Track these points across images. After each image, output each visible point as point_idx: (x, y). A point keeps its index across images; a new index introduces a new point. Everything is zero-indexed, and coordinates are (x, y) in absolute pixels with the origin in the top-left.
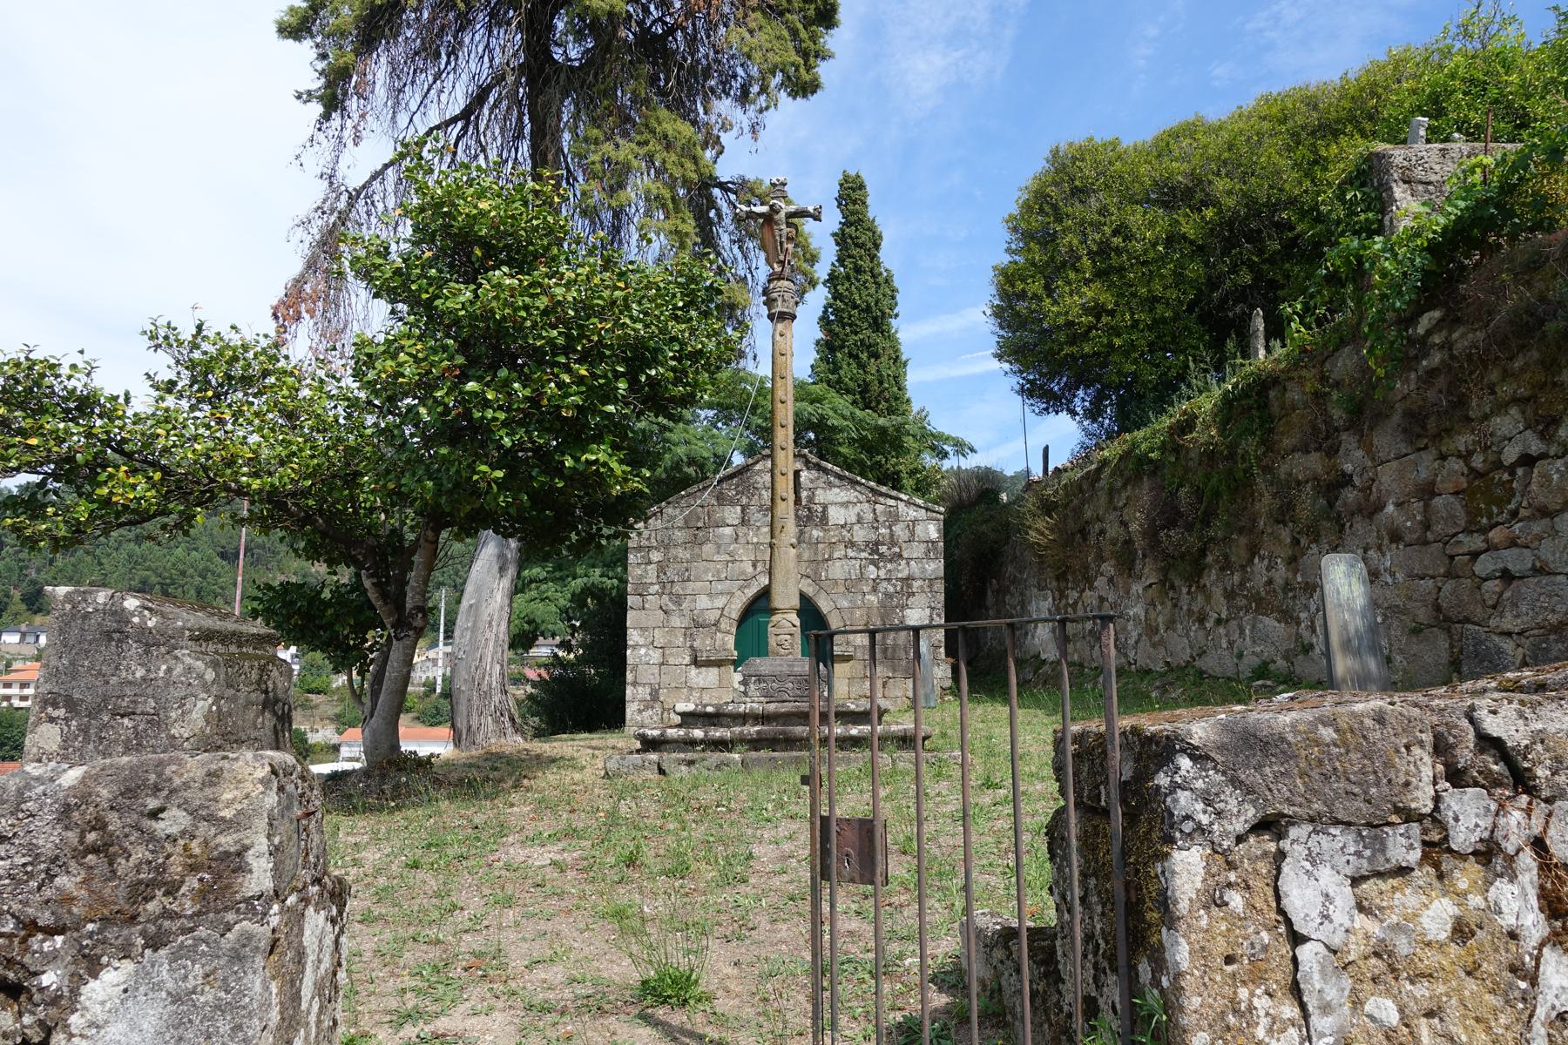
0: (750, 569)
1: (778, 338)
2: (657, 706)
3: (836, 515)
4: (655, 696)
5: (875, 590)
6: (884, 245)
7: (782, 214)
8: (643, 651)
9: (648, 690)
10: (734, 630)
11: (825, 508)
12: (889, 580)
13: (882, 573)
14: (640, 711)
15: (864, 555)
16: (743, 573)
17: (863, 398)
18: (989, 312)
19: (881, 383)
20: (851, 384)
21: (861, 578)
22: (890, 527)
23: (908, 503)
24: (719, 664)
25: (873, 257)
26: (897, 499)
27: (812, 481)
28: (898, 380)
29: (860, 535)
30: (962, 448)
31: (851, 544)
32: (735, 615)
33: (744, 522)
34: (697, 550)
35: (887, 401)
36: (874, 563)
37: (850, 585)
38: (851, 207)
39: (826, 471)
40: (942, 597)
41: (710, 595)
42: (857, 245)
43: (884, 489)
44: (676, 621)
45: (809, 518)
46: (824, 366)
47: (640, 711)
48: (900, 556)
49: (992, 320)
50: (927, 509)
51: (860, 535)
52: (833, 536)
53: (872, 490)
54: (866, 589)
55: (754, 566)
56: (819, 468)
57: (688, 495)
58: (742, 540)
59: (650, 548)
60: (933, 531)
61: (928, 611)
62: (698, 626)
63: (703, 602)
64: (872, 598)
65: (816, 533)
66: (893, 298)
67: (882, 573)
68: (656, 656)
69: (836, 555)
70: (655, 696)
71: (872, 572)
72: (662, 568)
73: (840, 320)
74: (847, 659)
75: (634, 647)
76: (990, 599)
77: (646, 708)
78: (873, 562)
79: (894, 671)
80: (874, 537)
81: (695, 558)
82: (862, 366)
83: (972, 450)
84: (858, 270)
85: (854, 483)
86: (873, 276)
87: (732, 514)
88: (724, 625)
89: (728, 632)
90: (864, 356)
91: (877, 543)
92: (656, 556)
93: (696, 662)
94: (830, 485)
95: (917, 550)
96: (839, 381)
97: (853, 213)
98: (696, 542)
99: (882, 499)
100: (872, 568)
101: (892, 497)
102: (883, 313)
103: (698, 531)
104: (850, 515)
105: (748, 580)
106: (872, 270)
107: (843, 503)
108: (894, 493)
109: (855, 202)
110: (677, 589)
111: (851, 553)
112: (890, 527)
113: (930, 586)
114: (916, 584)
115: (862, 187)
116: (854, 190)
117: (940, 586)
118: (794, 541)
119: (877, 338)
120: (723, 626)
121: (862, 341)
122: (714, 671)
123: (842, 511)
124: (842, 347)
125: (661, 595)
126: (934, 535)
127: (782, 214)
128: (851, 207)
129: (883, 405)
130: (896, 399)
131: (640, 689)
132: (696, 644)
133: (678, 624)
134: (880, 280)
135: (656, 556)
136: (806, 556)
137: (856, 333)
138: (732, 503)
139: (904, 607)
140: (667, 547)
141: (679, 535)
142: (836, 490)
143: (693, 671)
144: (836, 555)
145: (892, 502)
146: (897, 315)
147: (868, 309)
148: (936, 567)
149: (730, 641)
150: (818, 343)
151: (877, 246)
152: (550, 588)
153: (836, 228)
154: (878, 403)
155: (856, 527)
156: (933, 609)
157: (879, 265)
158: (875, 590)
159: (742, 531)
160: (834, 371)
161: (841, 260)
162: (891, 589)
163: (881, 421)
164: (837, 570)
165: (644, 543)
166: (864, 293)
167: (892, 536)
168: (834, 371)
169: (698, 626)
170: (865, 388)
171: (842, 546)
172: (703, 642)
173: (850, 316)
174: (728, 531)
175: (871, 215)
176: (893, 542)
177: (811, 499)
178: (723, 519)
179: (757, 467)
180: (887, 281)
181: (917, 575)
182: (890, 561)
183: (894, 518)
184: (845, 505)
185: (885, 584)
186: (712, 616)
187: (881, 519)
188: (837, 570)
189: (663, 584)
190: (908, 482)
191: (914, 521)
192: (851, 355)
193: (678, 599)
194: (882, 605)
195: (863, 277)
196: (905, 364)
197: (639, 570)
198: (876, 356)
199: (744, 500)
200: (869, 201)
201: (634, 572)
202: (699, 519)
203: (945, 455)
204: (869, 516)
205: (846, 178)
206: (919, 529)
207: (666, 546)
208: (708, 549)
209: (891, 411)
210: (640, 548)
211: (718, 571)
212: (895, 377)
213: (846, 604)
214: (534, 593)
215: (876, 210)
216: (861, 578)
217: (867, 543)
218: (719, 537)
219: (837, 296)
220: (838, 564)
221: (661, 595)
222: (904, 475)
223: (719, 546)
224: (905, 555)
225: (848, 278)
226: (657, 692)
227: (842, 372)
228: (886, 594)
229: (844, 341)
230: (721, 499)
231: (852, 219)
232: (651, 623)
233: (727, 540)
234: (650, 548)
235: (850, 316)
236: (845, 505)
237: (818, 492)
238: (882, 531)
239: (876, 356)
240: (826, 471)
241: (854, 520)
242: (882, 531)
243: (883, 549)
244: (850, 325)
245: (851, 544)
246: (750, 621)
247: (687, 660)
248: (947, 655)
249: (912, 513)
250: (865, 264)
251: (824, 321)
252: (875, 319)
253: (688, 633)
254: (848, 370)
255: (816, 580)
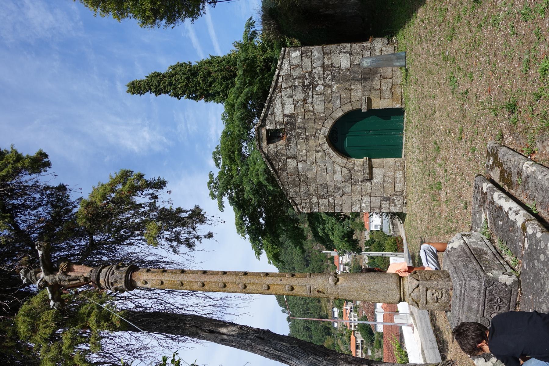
0: (320, 153)
1: (148, 286)
2: (392, 197)
3: (289, 109)
4: (387, 199)
5: (330, 86)
6: (158, 71)
7: (47, 278)
8: (364, 205)
9: (384, 202)
10: (354, 159)
11: (285, 116)
12: (324, 78)
13: (321, 82)
14: (395, 206)
15: (310, 93)
16: (322, 157)
17: (230, 79)
18: (172, 25)
19: (222, 70)
20: (224, 85)
21: (323, 94)
22: (294, 79)
23: (280, 69)
24: (371, 168)
25: (164, 77)
26: (278, 76)
27: (271, 123)
28: (220, 61)
29: (299, 96)
30: (250, 24)
31: (305, 100)
32: (345, 160)
33: (295, 157)
34: (311, 180)
35: (230, 67)
36: (315, 87)
37: (328, 100)
38: (142, 89)
39: (266, 116)
40: (334, 47)
41: (334, 173)
42: (159, 85)
43: (273, 84)
44: (348, 189)
45: (291, 124)
46: (217, 98)
47: (395, 206)
48: (310, 72)
49: (177, 23)
50: (283, 58)
51: (299, 96)
52: (300, 110)
53: (274, 90)
54: (330, 91)
55: (318, 151)
56: (264, 120)
57: (283, 185)
58: (305, 158)
59: (310, 202)
60: (296, 54)
61: (342, 55)
62: (350, 178)
63: (338, 176)
64: (335, 88)
65: (299, 120)
66: (182, 65)
67: (321, 82)
68: (366, 199)
69: (311, 109)
70: (387, 199)
71: (320, 88)
72: (322, 197)
73: (195, 91)
74: (369, 101)
75: (361, 209)
76: (331, 12)
77: (393, 203)
78: (315, 88)
79: (377, 73)
80: (300, 88)
81: (315, 181)
82: (215, 80)
83: (251, 19)
84: (170, 84)
85: (271, 101)
86: (173, 76)
87: (291, 163)
88: (351, 166)
89: (354, 164)
90: (210, 79)
91: (304, 86)
92: (315, 200)
93: (370, 179)
94: (273, 113)
95: (307, 63)
96: (223, 91)
97: (145, 88)
98: (307, 181)
99: (279, 84)
100: (318, 88)
101: (278, 79)
102: (189, 70)
103: (301, 180)
104: (289, 102)
105: (326, 154)
106: (170, 77)
107: (282, 107)
108: (275, 78)
109: (140, 87)
110: (331, 189)
111: (310, 100)
112: (294, 79)
113: (327, 54)
114: (327, 62)
115: (133, 83)
116: (135, 87)
117: (327, 48)
118: (331, 280)
119: (201, 74)
120: (351, 166)
121: (203, 81)
122: (375, 170)
123: (287, 106)
124: (207, 90)
125: (334, 197)
126: (298, 53)
127: (47, 278)
128: (142, 89)
129: (232, 68)
130: (229, 62)
131: (383, 206)
132: (360, 180)
133: (350, 188)
134: (174, 72)
135: (315, 200)
136: (312, 125)
137: (200, 84)
138: (286, 163)
139: (340, 69)
140: (310, 195)
141: (303, 189)
142: (276, 110)
143: (375, 180)
144: (311, 109)
145: (280, 78)
146: (190, 63)
147: (188, 78)
148: (316, 51)
149: (359, 161)
150: (207, 101)
151: (159, 75)
152: (328, 227)
153: (153, 95)
154: (231, 71)
155: (295, 98)
156: (340, 52)
157: (167, 73)
158: (330, 86)
159: (299, 158)
160: (218, 93)
161: (167, 92)
162: (329, 77)
163: (240, 73)
164: (319, 107)
165: (308, 205)
166: (181, 81)
167: (299, 78)
168: (218, 93)
169: (350, 178)
170: (225, 78)
171: (306, 106)
172: (359, 176)
173: (192, 87)
174: (300, 165)
175: (145, 78)
176: (303, 77)
177: (281, 123)
178: (294, 168)
179: (266, 152)
180: (174, 69)
181: (321, 62)
182: (313, 78)
183: (289, 77)
184: (283, 105)
185: (327, 81)
186: (345, 172)
187: (290, 84)
188: (319, 107)
189: (328, 197)
190: (269, 54)
191: (290, 65)
192: (210, 86)
193: (336, 189)
194: (338, 82)
195: (174, 82)
196: (212, 57)
197: (321, 207)
198: (209, 73)
199: (284, 158)
200: (139, 79)
201: (323, 209)
202: (294, 180)
203: (254, 32)
204: (289, 91)
205: (130, 91)
206: (295, 62)
207: (309, 195)
208: (310, 175)
209: (235, 64)
210: (311, 207)
211: (322, 170)
212: (219, 63)
213: (338, 102)
214: (330, 233)
215: (142, 75)
216: (323, 94)
217: (304, 92)
218: (303, 169)
219: (183, 93)
220: (316, 107)
221: (334, 197)
222: (265, 56)
223: (308, 170)
224: (310, 70)
225: (175, 89)
226: (385, 198)
227: (219, 90)
228: (333, 79)
229: (204, 90)
230: (284, 169)
231: (147, 88)
232: (349, 201)
233: (305, 165)
234: (310, 202)
235: (192, 87)
236: (283, 105)
237: (277, 119)
238: (297, 83)
239: (209, 73)
240: (266, 116)
241: (291, 100)
242: (297, 83)
243: (307, 82)
244: (196, 87)
245: (305, 100)
246: (349, 153)
247: (369, 184)
248: (366, 40)
249: (286, 67)
250: (167, 80)
251: (196, 98)
252: (192, 74)
253: (355, 183)
254: (217, 87)
255: (325, 119)
